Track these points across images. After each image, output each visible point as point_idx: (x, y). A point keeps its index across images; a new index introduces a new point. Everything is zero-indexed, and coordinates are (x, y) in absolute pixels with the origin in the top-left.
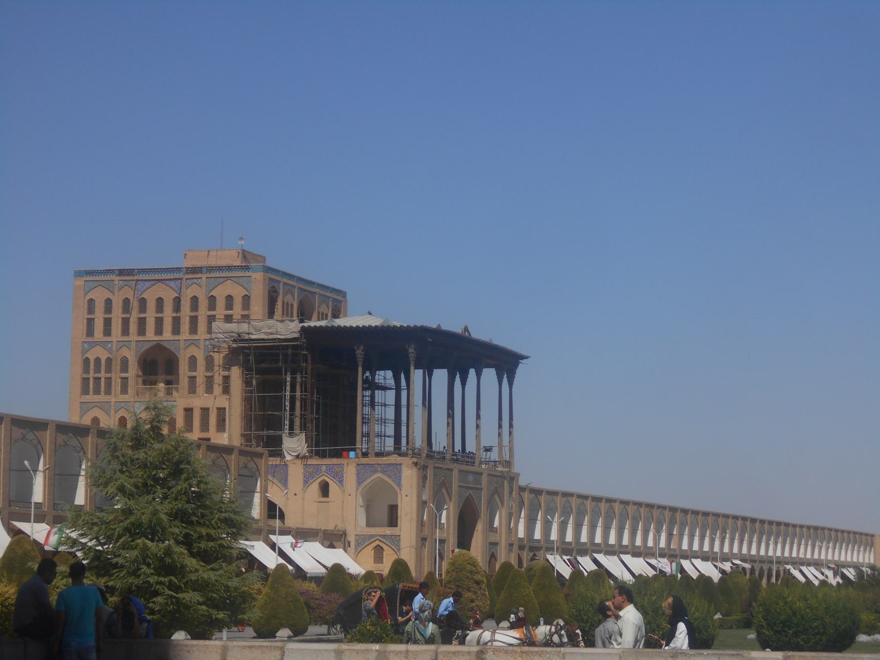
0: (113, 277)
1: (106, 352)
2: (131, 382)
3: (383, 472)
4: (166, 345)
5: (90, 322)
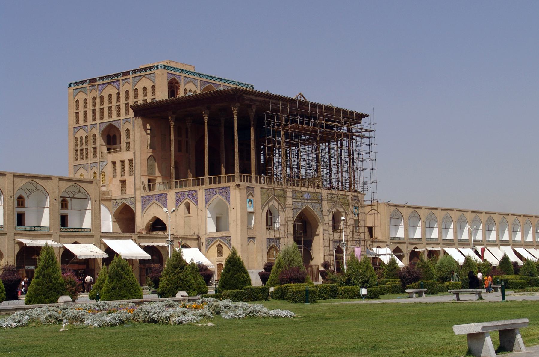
0: (86, 85)
1: (85, 133)
3: (220, 193)
4: (113, 123)
5: (77, 114)
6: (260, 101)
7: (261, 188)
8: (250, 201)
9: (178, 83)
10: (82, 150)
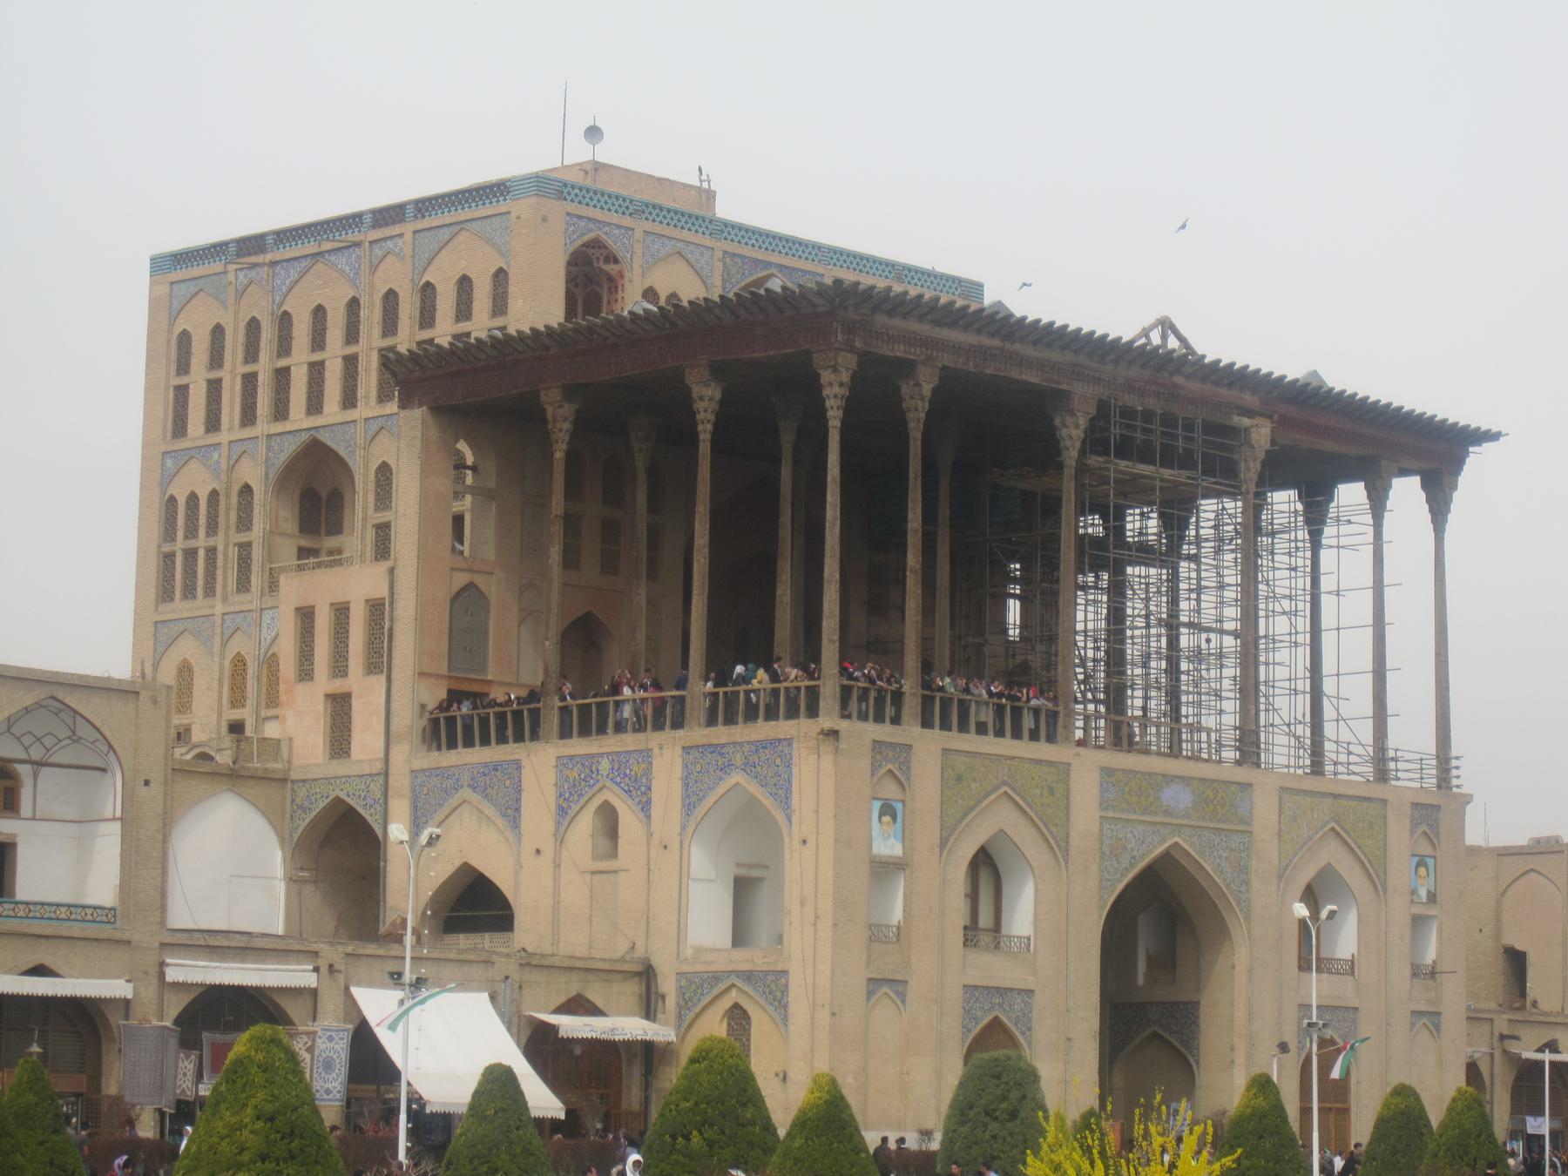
0: (217, 267)
2: (257, 553)
4: (326, 438)
5: (182, 392)
6: (957, 349)
7: (945, 751)
8: (888, 810)
9: (616, 261)
10: (191, 554)
